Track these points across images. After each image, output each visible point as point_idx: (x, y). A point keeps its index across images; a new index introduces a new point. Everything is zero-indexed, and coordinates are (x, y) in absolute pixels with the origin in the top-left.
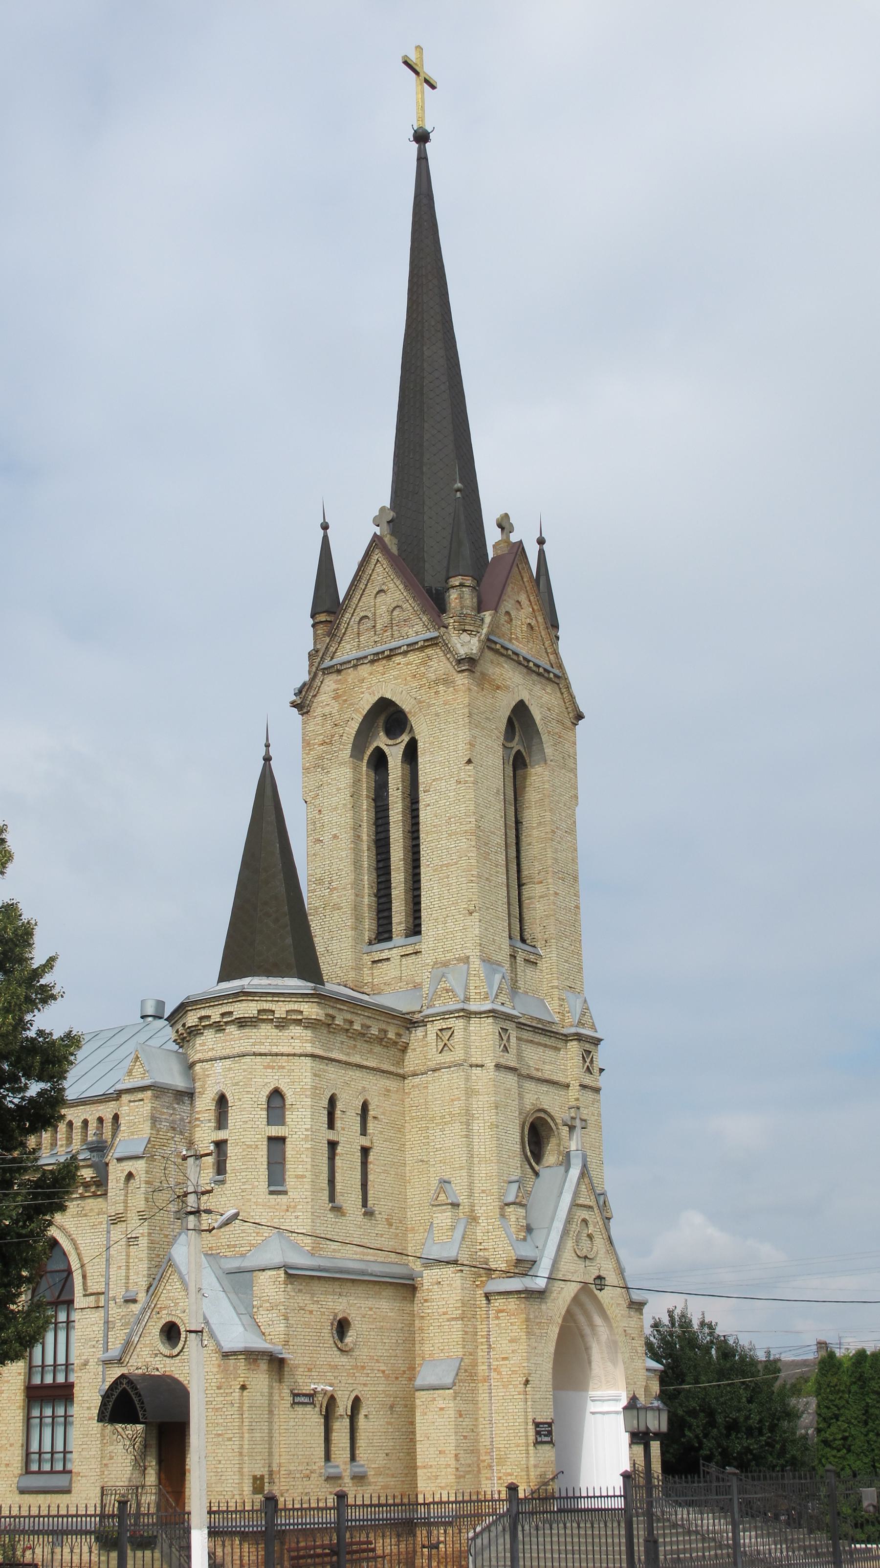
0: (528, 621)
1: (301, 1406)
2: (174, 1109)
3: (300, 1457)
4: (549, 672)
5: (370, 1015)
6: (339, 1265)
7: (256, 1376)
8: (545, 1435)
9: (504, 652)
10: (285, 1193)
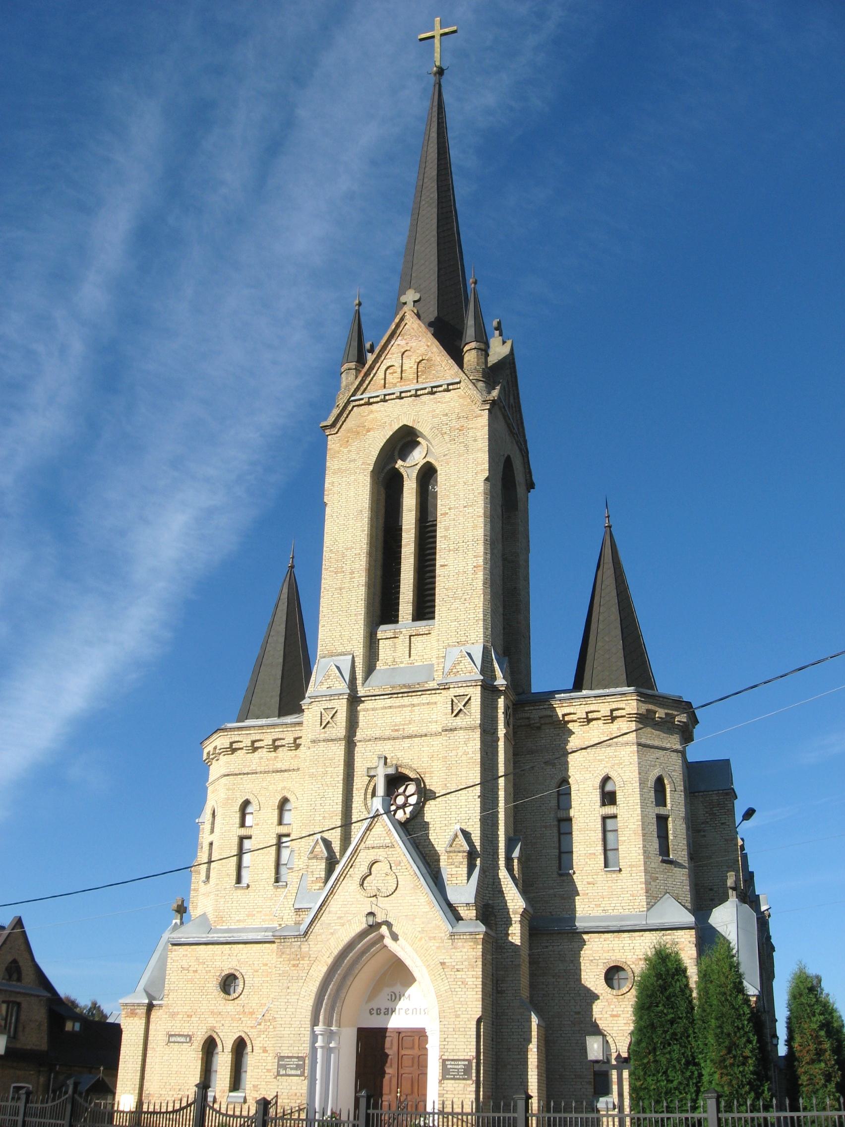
1: (177, 1044)
3: (172, 1084)
4: (441, 386)
5: (281, 730)
7: (133, 1021)
8: (291, 1069)
9: (378, 399)
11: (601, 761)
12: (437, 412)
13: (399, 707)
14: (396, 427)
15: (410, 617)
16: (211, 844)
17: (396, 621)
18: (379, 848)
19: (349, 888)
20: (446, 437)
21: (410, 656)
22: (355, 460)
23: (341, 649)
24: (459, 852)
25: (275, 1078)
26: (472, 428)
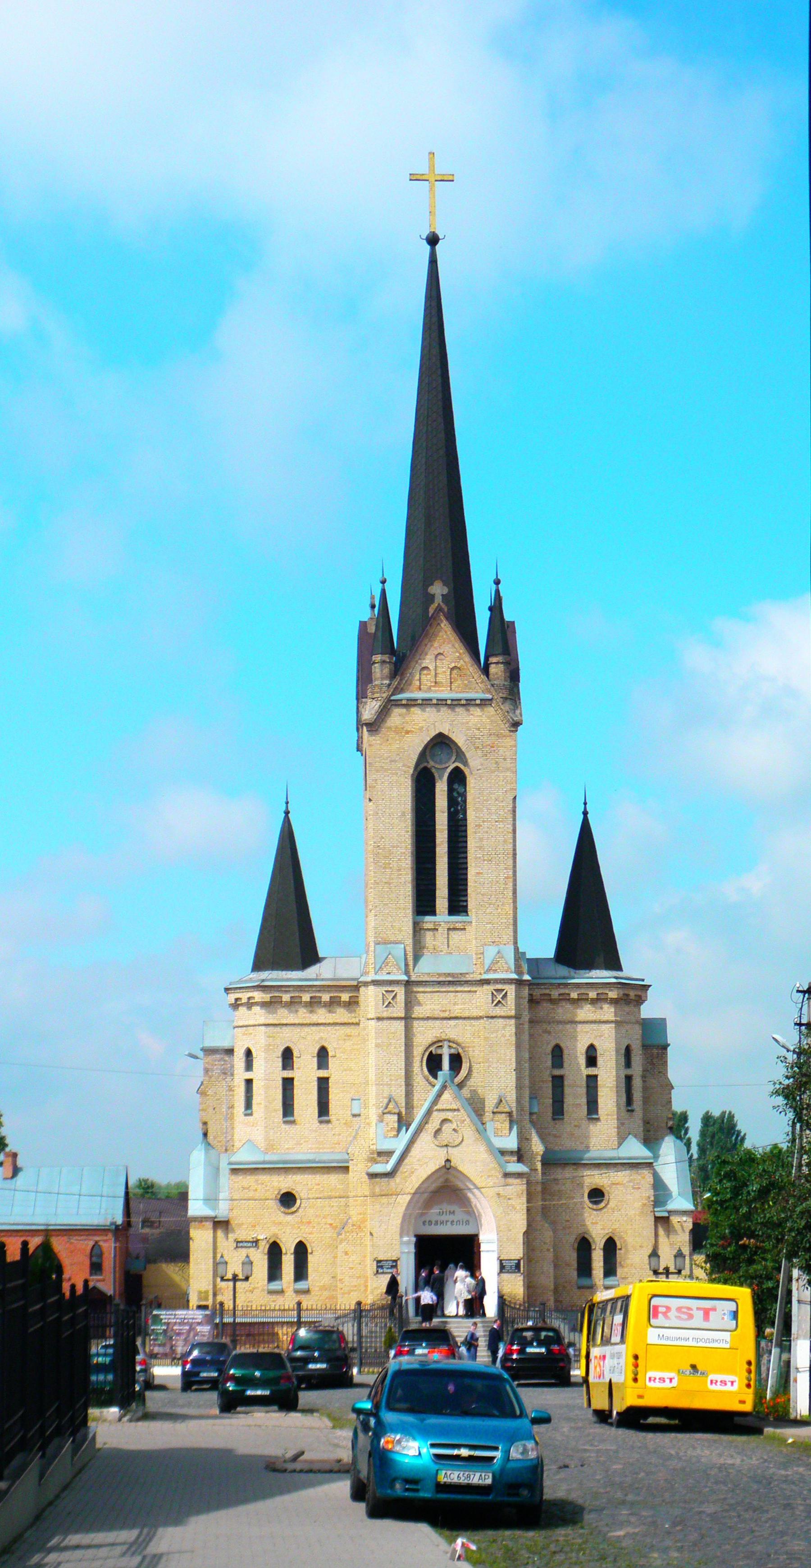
0: (453, 665)
2: (225, 1061)
4: (475, 700)
6: (288, 1159)
8: (388, 1268)
10: (251, 1114)
11: (587, 1032)
12: (470, 724)
13: (445, 992)
14: (433, 733)
15: (447, 912)
16: (249, 1082)
17: (433, 913)
18: (448, 1110)
19: (426, 1138)
20: (479, 752)
21: (448, 946)
22: (395, 761)
23: (393, 939)
24: (503, 1113)
25: (375, 1275)
26: (502, 746)
